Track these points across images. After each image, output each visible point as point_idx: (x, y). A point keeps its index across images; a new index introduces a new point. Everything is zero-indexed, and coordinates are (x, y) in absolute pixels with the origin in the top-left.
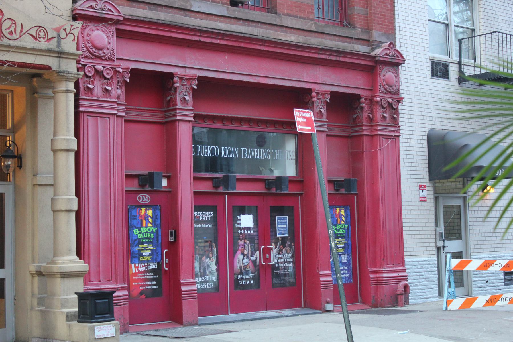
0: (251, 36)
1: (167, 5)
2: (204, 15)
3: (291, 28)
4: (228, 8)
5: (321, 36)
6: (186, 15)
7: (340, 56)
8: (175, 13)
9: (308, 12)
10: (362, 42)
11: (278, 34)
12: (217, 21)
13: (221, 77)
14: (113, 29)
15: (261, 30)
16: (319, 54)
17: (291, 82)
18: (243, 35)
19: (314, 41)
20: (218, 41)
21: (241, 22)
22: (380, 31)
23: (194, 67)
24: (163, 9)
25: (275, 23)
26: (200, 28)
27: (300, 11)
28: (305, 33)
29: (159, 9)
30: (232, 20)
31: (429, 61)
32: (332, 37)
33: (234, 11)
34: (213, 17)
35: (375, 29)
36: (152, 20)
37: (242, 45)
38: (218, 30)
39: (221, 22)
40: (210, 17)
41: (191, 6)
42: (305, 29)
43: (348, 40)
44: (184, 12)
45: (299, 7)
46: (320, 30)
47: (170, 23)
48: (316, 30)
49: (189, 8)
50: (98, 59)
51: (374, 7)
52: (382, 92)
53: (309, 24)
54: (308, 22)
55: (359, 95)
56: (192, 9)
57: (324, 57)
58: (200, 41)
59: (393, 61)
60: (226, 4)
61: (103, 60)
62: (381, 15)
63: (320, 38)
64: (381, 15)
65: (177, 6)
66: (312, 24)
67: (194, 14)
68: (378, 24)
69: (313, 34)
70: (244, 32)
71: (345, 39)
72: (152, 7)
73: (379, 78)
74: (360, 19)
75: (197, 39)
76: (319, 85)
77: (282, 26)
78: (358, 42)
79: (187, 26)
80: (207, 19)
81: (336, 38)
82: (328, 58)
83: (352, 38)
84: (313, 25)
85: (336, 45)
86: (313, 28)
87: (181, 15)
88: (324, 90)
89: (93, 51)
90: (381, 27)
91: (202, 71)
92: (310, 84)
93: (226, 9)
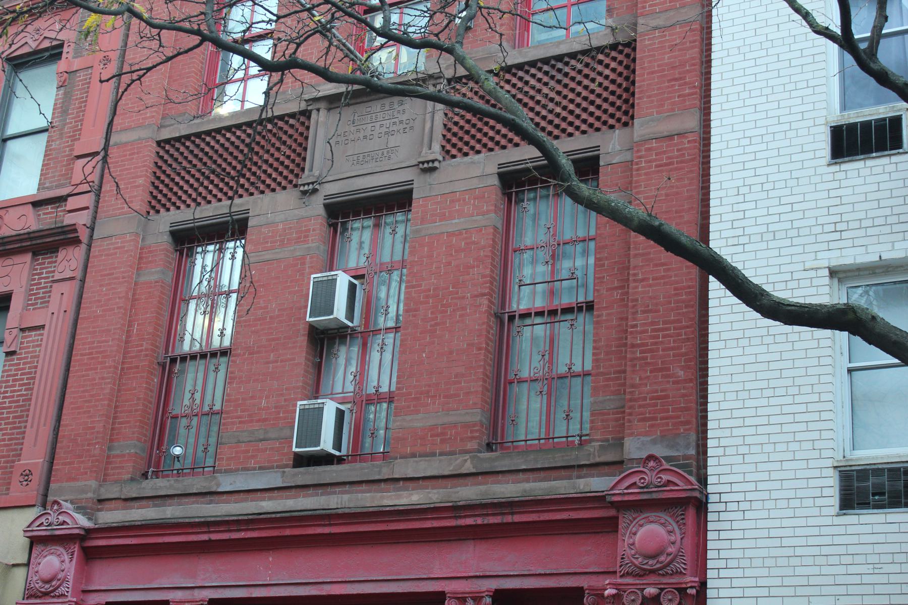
0: (381, 509)
1: (179, 492)
2: (242, 496)
3: (418, 479)
4: (284, 472)
5: (491, 479)
6: (210, 502)
7: (512, 514)
8: (193, 503)
9: (462, 440)
10: (606, 469)
11: (382, 498)
12: (263, 499)
13: (254, 596)
14: (76, 548)
15: (346, 497)
16: (455, 517)
17: (401, 584)
18: (278, 515)
19: (468, 493)
20: (242, 535)
21: (311, 491)
22: (646, 434)
23: (206, 585)
24: (176, 500)
25: (377, 477)
26: (203, 520)
27: (442, 441)
28: (449, 482)
29: (170, 501)
30: (293, 492)
31: (831, 472)
32: (521, 476)
33: (295, 475)
34: (259, 494)
35: (631, 435)
36: (127, 524)
37: (288, 532)
38: (260, 514)
39: (270, 499)
40: (251, 496)
41: (218, 485)
42: (446, 473)
43: (563, 473)
44: (208, 498)
45: (443, 434)
46: (486, 467)
47: (149, 522)
48: (474, 471)
49: (213, 490)
50: (47, 597)
51: (633, 386)
52: (628, 574)
53: (458, 461)
54: (456, 460)
55: (582, 587)
56: (220, 490)
57: (470, 521)
58: (210, 541)
59: (654, 496)
60: (286, 466)
61: (53, 597)
62: (652, 399)
63: (487, 483)
64: (652, 399)
65: (195, 491)
66: (466, 461)
67: (225, 497)
68: (640, 420)
69: (470, 480)
70: (309, 507)
71: (554, 474)
72: (157, 502)
73: (620, 543)
74: (603, 421)
75: (205, 537)
76: (469, 581)
77: (397, 480)
78: (594, 471)
79: (181, 520)
80: (246, 500)
81: (531, 475)
82: (486, 522)
83: (572, 467)
84: (469, 461)
85: (525, 491)
86: (468, 468)
87: (202, 503)
88: (478, 589)
89: (651, 565)
90: (652, 426)
91: (220, 590)
92: (447, 582)
93: (279, 475)
